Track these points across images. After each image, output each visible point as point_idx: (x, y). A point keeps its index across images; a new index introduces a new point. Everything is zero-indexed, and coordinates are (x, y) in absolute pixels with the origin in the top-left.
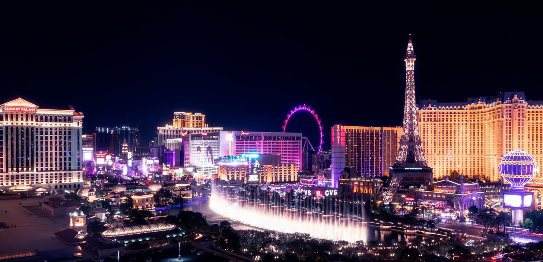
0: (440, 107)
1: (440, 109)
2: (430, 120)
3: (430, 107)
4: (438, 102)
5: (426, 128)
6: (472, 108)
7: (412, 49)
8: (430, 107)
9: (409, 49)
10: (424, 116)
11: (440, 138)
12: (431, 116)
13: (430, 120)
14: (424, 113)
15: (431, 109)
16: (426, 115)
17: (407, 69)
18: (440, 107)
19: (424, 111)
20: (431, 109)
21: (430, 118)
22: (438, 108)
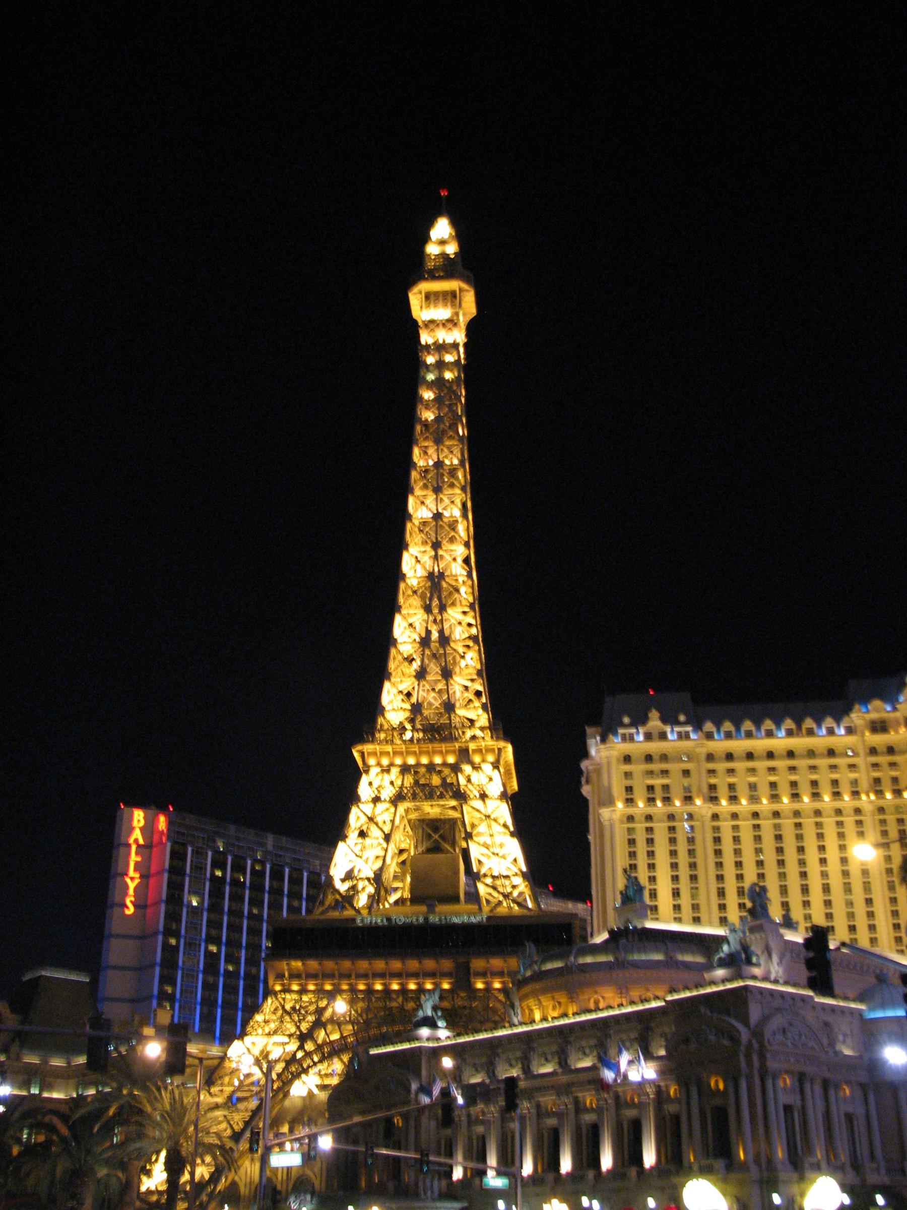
0: (709, 726)
1: (709, 736)
2: (659, 793)
3: (655, 722)
4: (696, 701)
5: (641, 838)
6: (879, 727)
7: (452, 249)
8: (655, 722)
9: (432, 249)
10: (628, 775)
11: (721, 893)
12: (665, 773)
13: (659, 793)
14: (627, 759)
15: (663, 736)
16: (637, 768)
17: (426, 338)
18: (709, 726)
19: (627, 747)
20: (663, 736)
21: (658, 782)
22: (698, 727)
